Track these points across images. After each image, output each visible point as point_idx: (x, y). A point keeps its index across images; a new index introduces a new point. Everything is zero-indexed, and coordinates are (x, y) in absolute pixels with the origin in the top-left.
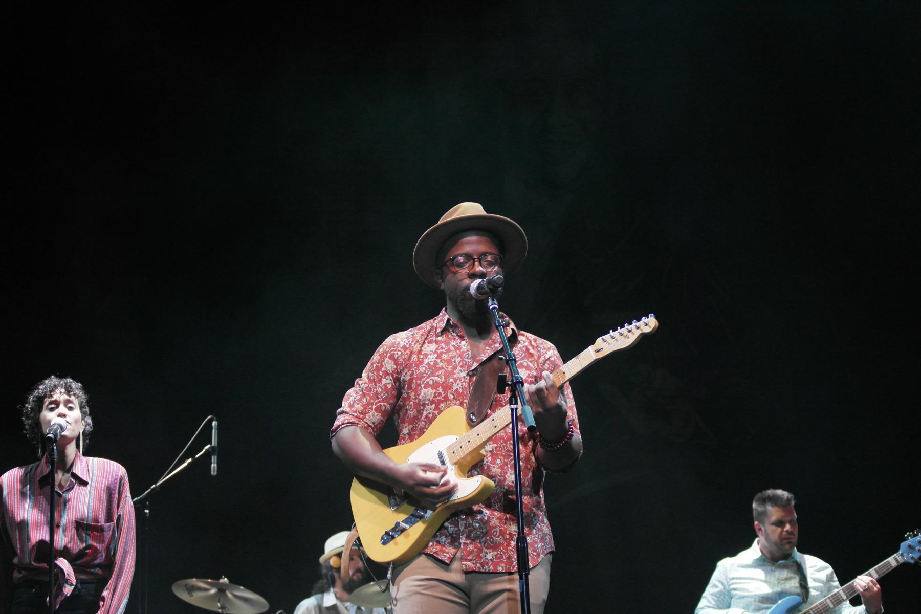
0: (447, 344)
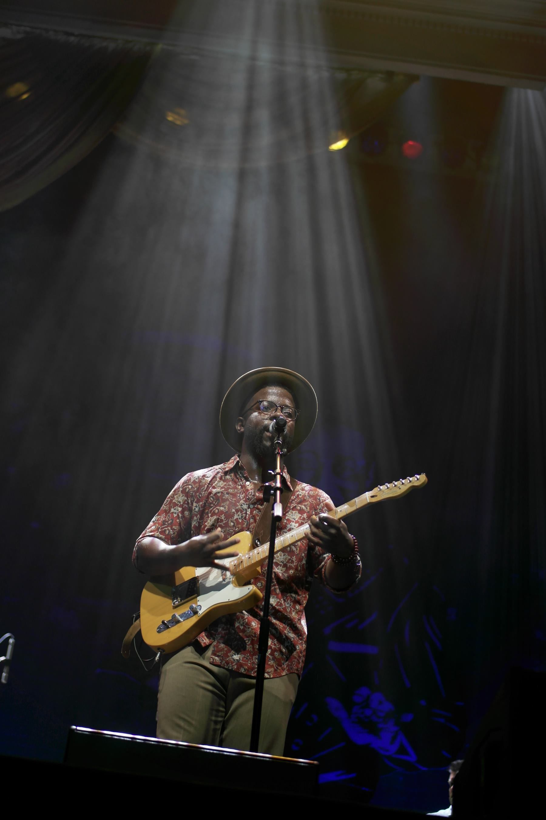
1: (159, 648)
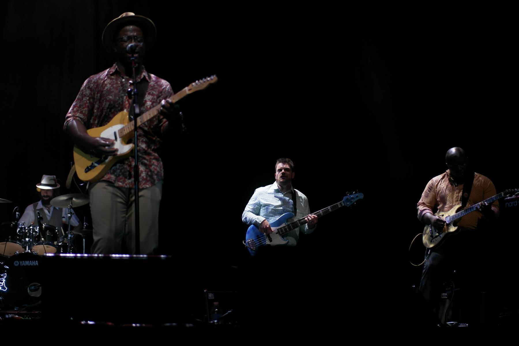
0: (117, 80)
1: (87, 182)
